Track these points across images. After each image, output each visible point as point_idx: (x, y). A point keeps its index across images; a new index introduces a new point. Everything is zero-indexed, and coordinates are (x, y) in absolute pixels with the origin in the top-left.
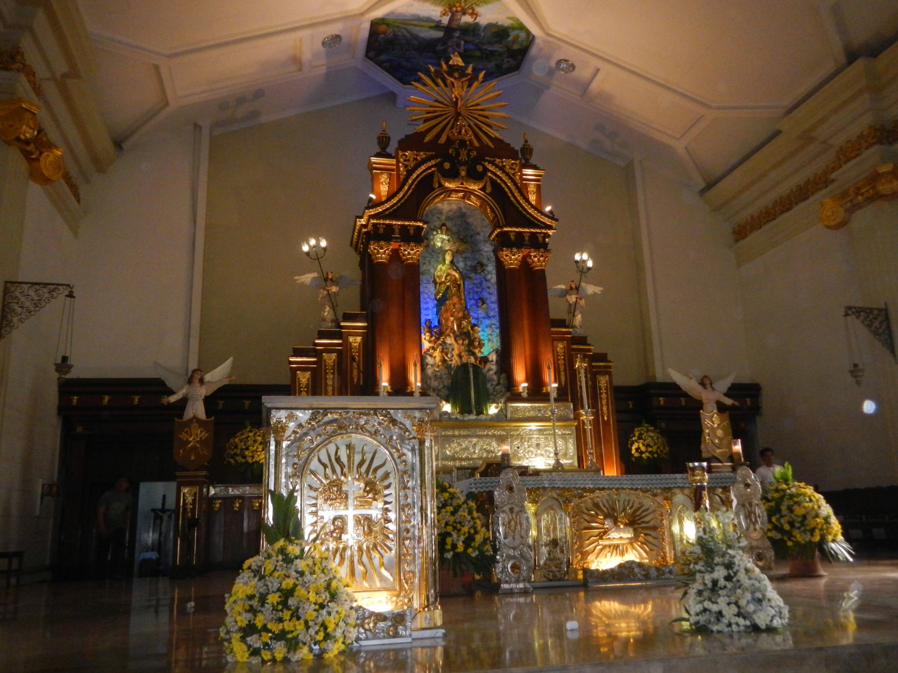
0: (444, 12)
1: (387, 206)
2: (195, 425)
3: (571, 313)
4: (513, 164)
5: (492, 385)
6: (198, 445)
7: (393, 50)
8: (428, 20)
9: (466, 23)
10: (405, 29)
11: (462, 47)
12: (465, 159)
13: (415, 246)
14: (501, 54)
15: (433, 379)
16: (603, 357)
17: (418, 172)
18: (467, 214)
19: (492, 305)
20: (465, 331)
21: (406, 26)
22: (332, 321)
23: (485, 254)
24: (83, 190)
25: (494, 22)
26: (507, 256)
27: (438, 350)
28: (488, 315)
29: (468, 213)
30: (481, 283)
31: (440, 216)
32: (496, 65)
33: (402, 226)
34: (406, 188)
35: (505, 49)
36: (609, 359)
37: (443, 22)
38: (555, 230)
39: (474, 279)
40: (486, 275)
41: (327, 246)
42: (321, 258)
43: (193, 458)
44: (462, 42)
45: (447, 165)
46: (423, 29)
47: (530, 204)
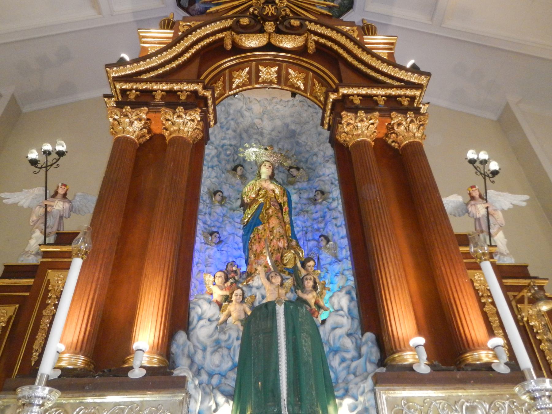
1: (143, 66)
3: (482, 231)
13: (186, 114)
15: (209, 350)
18: (298, 131)
19: (342, 240)
20: (290, 266)
23: (327, 178)
26: (348, 124)
27: (234, 298)
28: (336, 257)
29: (298, 128)
30: (324, 217)
31: (260, 138)
38: (428, 103)
39: (312, 214)
40: (331, 203)
42: (51, 165)
45: (245, 21)
47: (378, 58)
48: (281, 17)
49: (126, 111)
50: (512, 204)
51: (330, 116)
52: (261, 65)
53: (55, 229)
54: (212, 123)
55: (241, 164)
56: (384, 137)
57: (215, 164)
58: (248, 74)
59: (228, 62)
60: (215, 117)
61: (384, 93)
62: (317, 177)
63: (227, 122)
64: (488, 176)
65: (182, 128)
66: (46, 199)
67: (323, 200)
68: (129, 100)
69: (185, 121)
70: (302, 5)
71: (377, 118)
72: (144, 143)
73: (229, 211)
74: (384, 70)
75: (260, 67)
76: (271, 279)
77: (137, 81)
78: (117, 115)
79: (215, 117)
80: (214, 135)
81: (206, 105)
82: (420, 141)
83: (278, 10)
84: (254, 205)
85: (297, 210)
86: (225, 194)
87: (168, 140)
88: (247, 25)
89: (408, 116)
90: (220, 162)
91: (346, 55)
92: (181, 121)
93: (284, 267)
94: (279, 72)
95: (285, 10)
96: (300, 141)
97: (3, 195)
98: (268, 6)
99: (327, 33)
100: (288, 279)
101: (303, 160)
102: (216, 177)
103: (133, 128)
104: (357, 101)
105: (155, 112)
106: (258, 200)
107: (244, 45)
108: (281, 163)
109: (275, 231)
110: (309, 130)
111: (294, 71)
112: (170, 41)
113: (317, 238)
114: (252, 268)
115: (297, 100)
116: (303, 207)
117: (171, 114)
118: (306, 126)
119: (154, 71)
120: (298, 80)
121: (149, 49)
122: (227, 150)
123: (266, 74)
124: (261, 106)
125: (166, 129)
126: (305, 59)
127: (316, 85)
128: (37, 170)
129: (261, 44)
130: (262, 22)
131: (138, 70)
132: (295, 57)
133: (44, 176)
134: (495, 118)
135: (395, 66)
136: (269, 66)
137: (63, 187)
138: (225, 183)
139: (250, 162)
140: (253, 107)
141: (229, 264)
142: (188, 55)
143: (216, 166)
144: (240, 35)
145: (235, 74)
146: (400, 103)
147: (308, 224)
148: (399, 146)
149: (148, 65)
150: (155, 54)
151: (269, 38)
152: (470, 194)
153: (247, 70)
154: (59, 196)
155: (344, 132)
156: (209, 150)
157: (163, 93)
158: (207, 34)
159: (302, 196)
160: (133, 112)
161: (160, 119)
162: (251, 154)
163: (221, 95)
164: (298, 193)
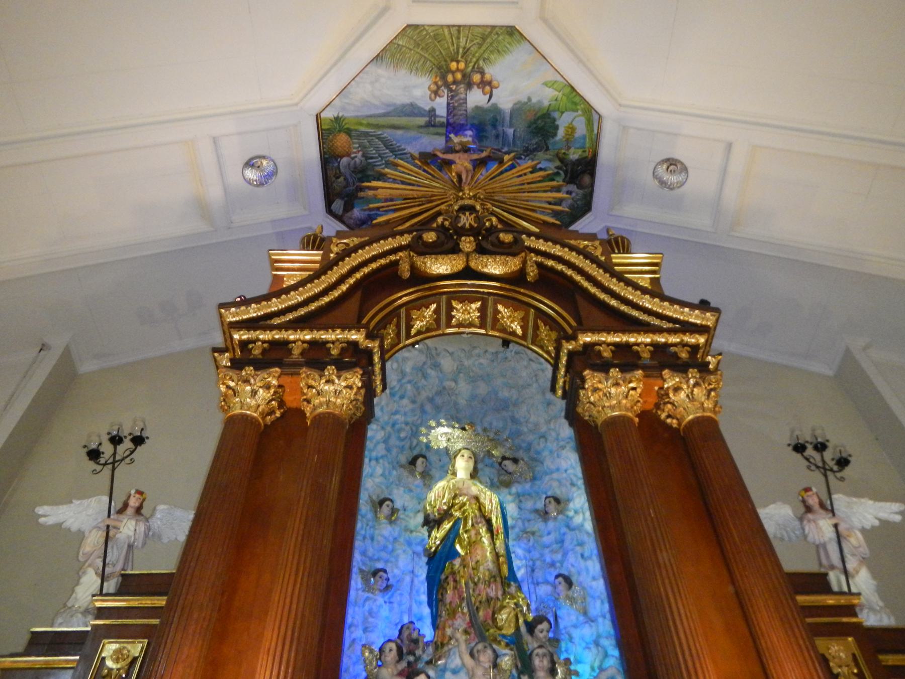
1: (276, 305)
8: (412, 110)
9: (477, 108)
10: (379, 137)
12: (470, 224)
13: (339, 377)
19: (594, 584)
21: (379, 133)
23: (564, 475)
26: (596, 390)
34: (332, 277)
35: (558, 163)
37: (438, 113)
38: (720, 354)
39: (541, 536)
40: (571, 518)
45: (430, 237)
47: (636, 286)
48: (484, 230)
49: (247, 374)
50: (877, 518)
51: (566, 376)
52: (455, 300)
53: (118, 568)
54: (379, 389)
55: (424, 454)
56: (653, 409)
57: (380, 455)
58: (435, 314)
59: (404, 297)
60: (384, 380)
61: (648, 340)
62: (546, 474)
63: (401, 386)
64: (831, 470)
65: (333, 399)
66: (109, 515)
67: (560, 512)
68: (252, 356)
69: (339, 388)
70: (515, 211)
71: (641, 381)
72: (273, 423)
73: (403, 533)
74: (647, 305)
75: (454, 303)
76: (476, 655)
77: (265, 328)
78: (233, 381)
79: (384, 380)
80: (379, 407)
81: (371, 363)
82: (713, 416)
83: (479, 219)
84: (446, 522)
85: (517, 530)
86: (398, 504)
87: (310, 418)
88: (434, 242)
89: (690, 376)
90: (388, 450)
91: (586, 284)
92: (332, 388)
93: (498, 632)
94: (482, 310)
95: (489, 220)
96: (517, 416)
97: (40, 510)
98: (465, 214)
99: (554, 252)
100: (505, 655)
101: (524, 445)
102: (382, 475)
103: (256, 401)
104: (607, 354)
105: (292, 374)
106: (452, 515)
107: (428, 271)
108: (488, 452)
109: (481, 568)
110: (531, 398)
111: (505, 307)
112: (317, 265)
113: (551, 578)
114: (444, 635)
115: (511, 351)
116: (526, 524)
117: (317, 377)
118: (528, 391)
119: (291, 312)
120: (512, 322)
121: (285, 279)
122: (399, 431)
123: (462, 313)
124: (454, 360)
125: (309, 401)
126: (522, 290)
127: (540, 329)
128: (99, 468)
129: (456, 270)
130: (455, 237)
131: (269, 310)
132: (507, 287)
133: (109, 477)
134: (831, 373)
135: (663, 298)
136: (466, 302)
137: (137, 496)
138: (397, 485)
139: (438, 450)
140: (442, 362)
141: (405, 629)
142: (344, 287)
143: (382, 457)
144: (423, 257)
145: (415, 314)
146: (675, 355)
147: (536, 554)
148: (679, 424)
149: (283, 304)
150: (295, 288)
151: (467, 261)
152: (804, 501)
153: (433, 307)
154: (130, 511)
155: (590, 402)
156: (374, 432)
157: (305, 345)
158: (373, 256)
159: (523, 505)
160: (257, 375)
161: (299, 385)
162: (439, 438)
163: (393, 346)
164: (517, 501)
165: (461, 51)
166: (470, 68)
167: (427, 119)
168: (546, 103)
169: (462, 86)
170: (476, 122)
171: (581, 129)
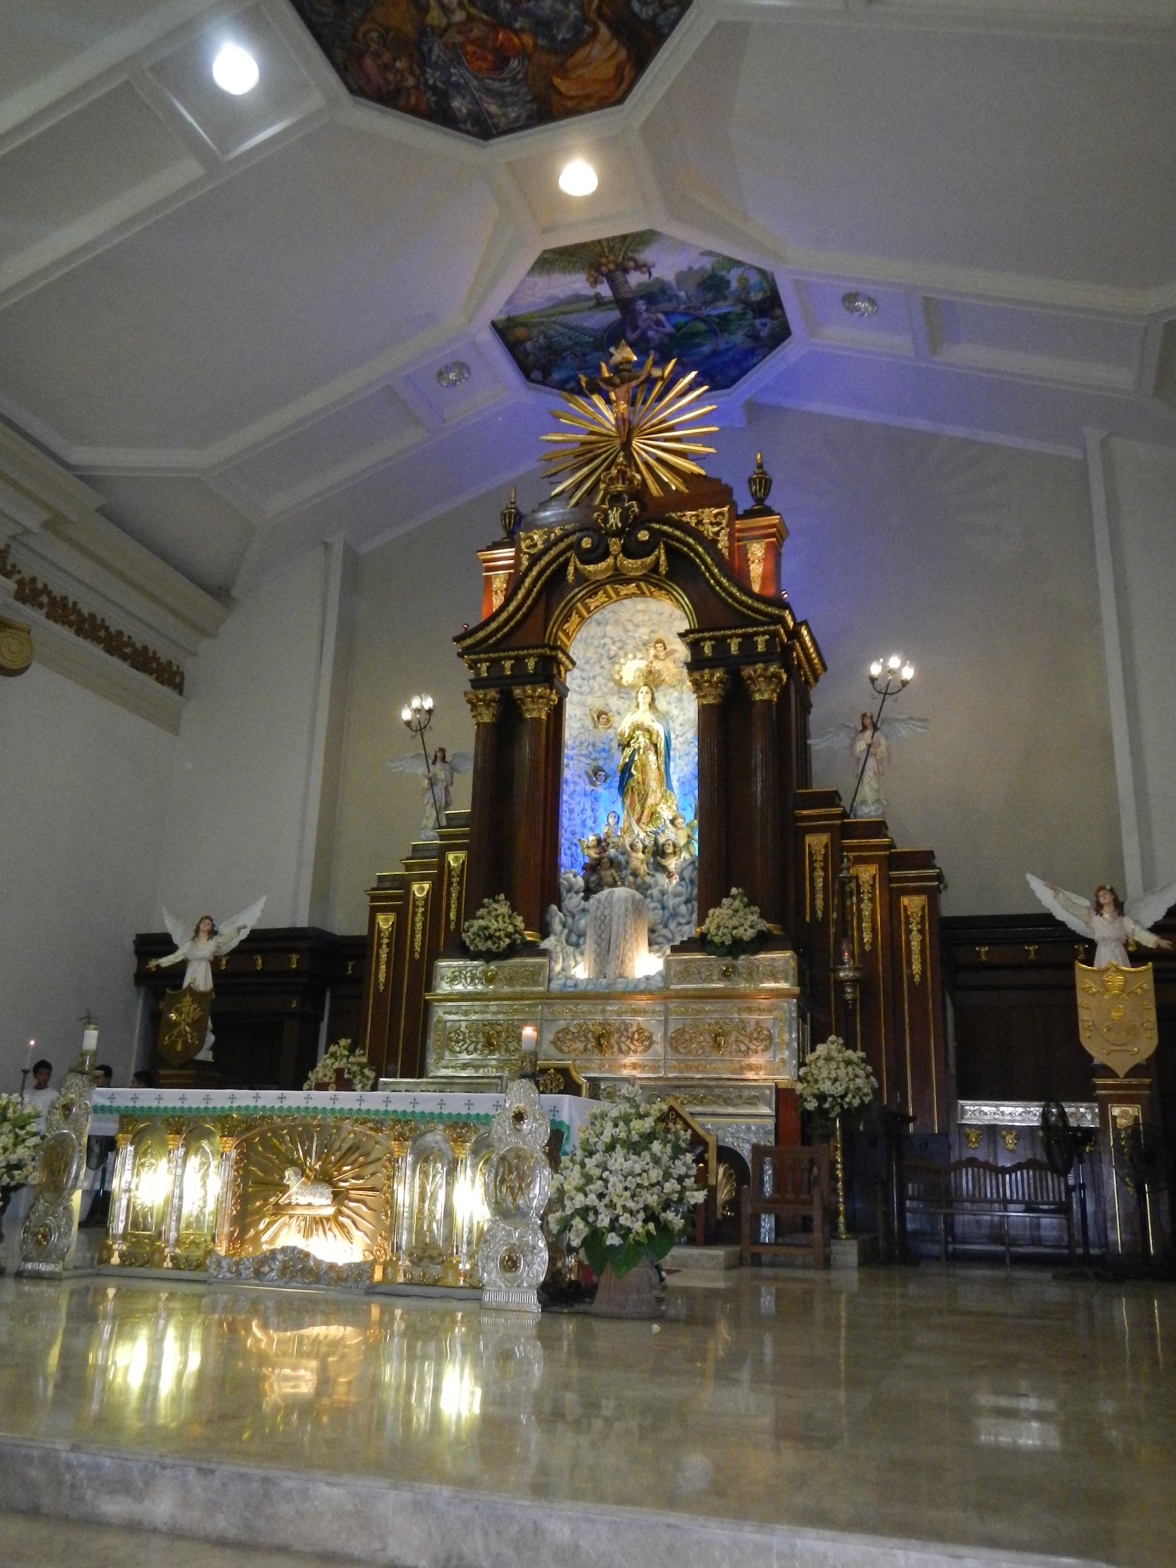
0: (592, 279)
2: (188, 998)
4: (716, 516)
5: (680, 924)
6: (188, 1029)
7: (564, 359)
8: (578, 298)
9: (640, 285)
10: (554, 322)
11: (667, 324)
14: (741, 317)
15: (577, 917)
16: (925, 858)
17: (543, 562)
21: (553, 319)
22: (434, 828)
24: (189, 667)
25: (684, 267)
32: (745, 335)
33: (516, 658)
34: (520, 595)
36: (937, 862)
37: (603, 295)
41: (434, 706)
42: (425, 727)
43: (179, 1048)
44: (661, 317)
45: (586, 543)
46: (582, 315)
86: (614, 709)
128: (414, 733)
165: (606, 250)
166: (620, 260)
167: (594, 301)
168: (708, 266)
169: (618, 273)
170: (643, 293)
171: (754, 278)
